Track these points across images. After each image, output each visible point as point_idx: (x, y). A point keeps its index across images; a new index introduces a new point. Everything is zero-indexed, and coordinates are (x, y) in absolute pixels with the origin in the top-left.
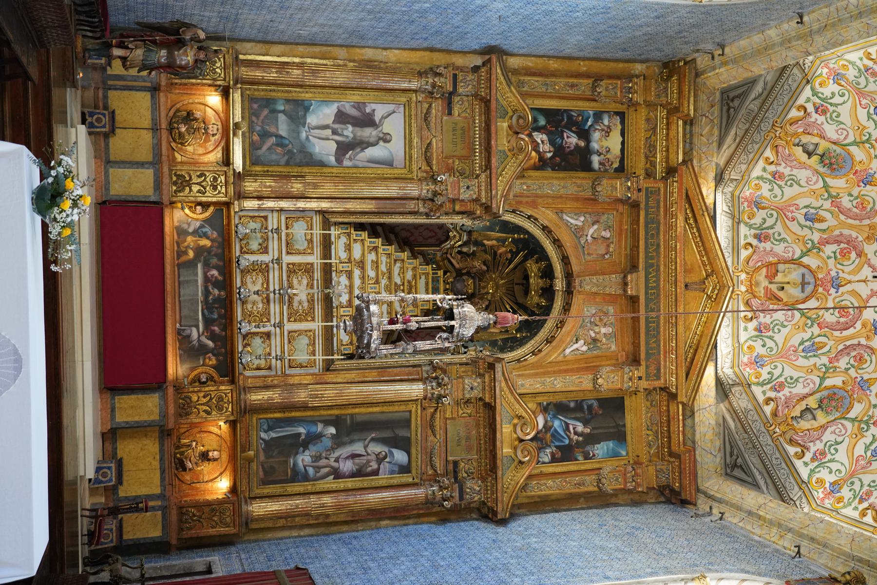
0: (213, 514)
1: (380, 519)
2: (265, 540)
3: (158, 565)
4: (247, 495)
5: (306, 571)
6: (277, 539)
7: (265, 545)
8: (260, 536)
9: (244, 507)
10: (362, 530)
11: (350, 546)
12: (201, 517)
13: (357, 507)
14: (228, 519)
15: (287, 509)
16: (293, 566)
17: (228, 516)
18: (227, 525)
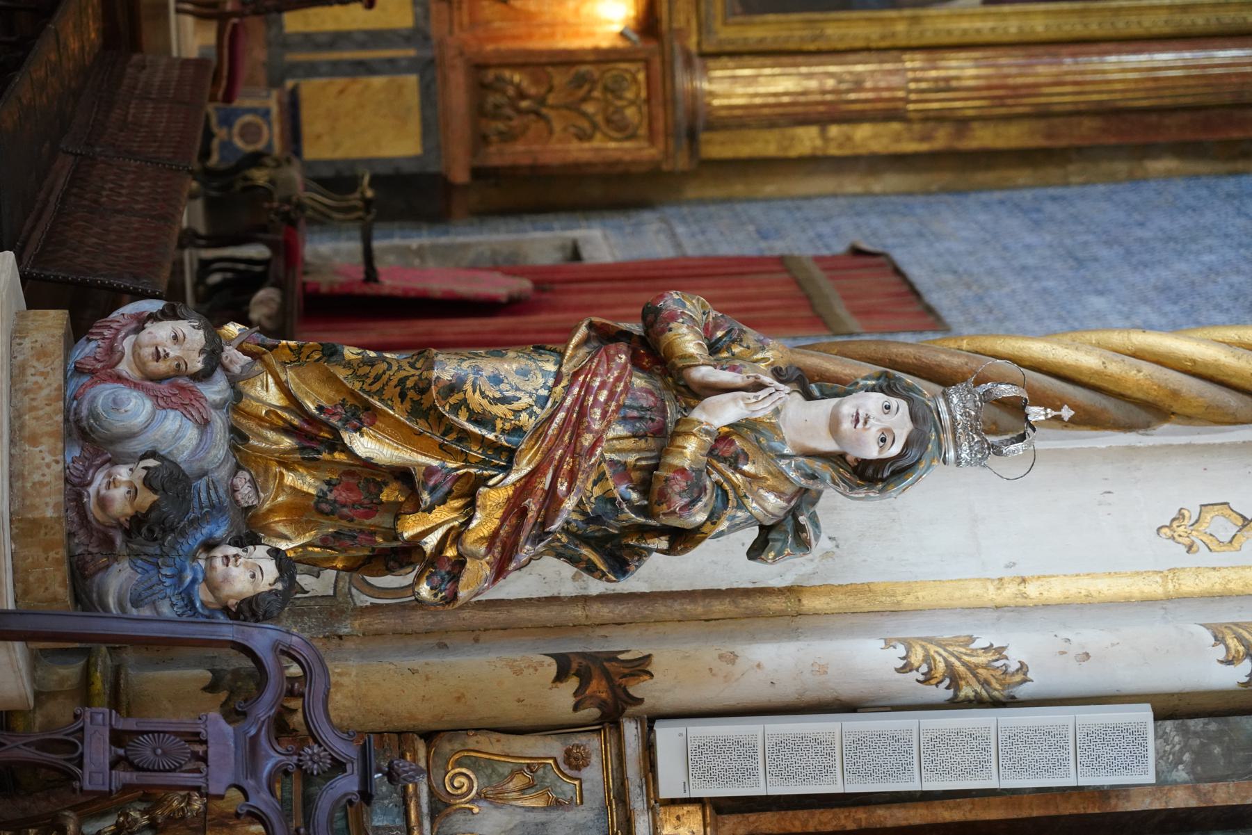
0: (582, 92)
1: (1146, 151)
2: (749, 200)
3: (414, 243)
4: (693, 46)
5: (881, 260)
6: (792, 198)
7: (756, 210)
8: (739, 189)
9: (683, 81)
10: (1084, 184)
11: (1035, 216)
12: (542, 101)
13: (1063, 98)
14: (630, 112)
15: (824, 92)
16: (840, 248)
17: (632, 103)
18: (624, 130)
